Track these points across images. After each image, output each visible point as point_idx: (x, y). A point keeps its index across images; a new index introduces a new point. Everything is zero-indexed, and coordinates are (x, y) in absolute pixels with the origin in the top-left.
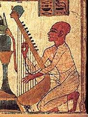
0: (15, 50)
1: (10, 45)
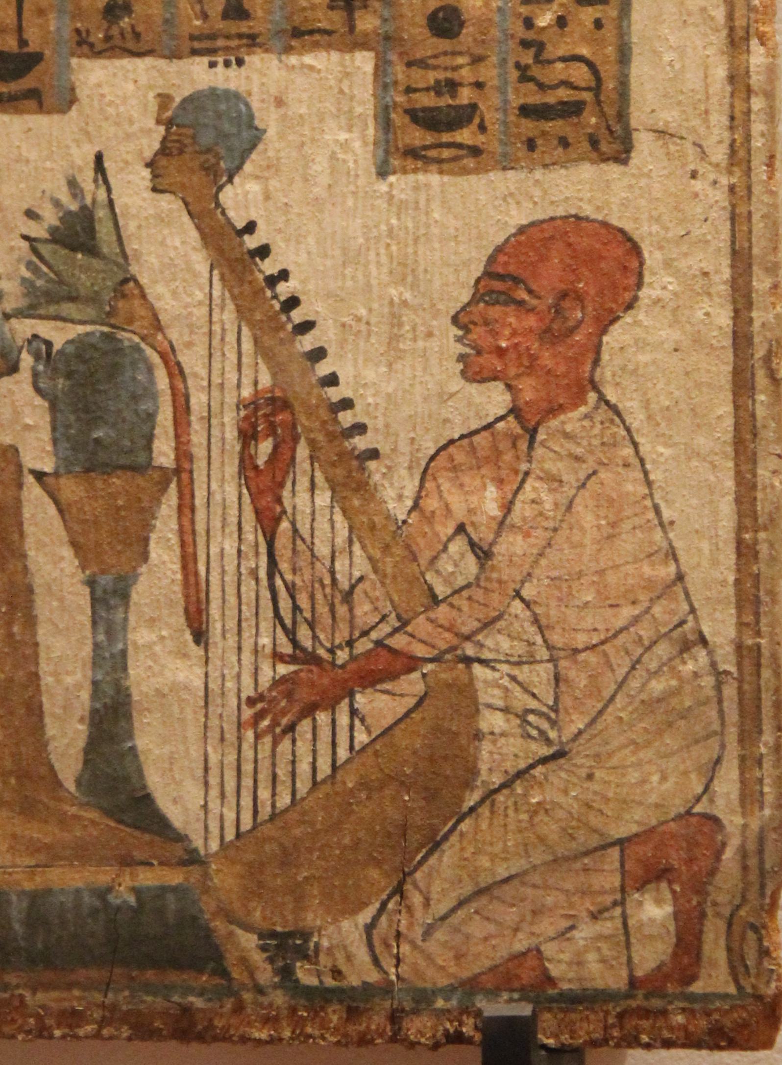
0: (183, 454)
1: (151, 417)
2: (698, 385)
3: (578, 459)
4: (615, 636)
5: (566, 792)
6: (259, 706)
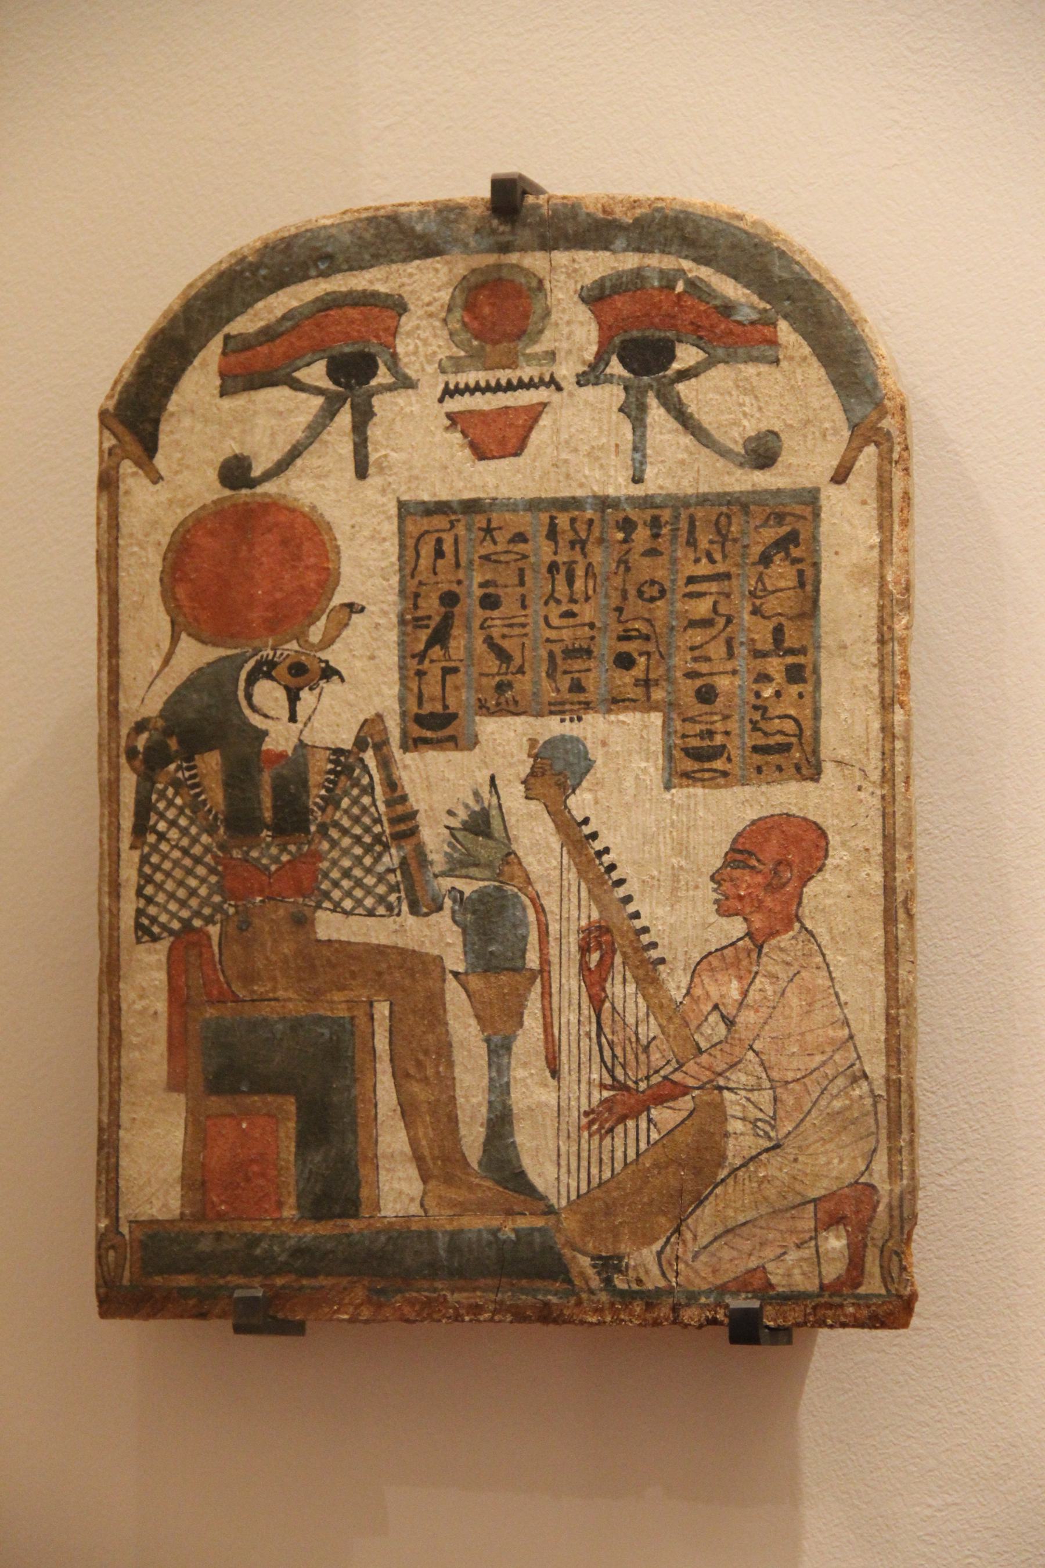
0: (544, 961)
1: (525, 938)
2: (862, 918)
3: (788, 964)
4: (811, 1073)
5: (781, 1170)
6: (592, 1116)
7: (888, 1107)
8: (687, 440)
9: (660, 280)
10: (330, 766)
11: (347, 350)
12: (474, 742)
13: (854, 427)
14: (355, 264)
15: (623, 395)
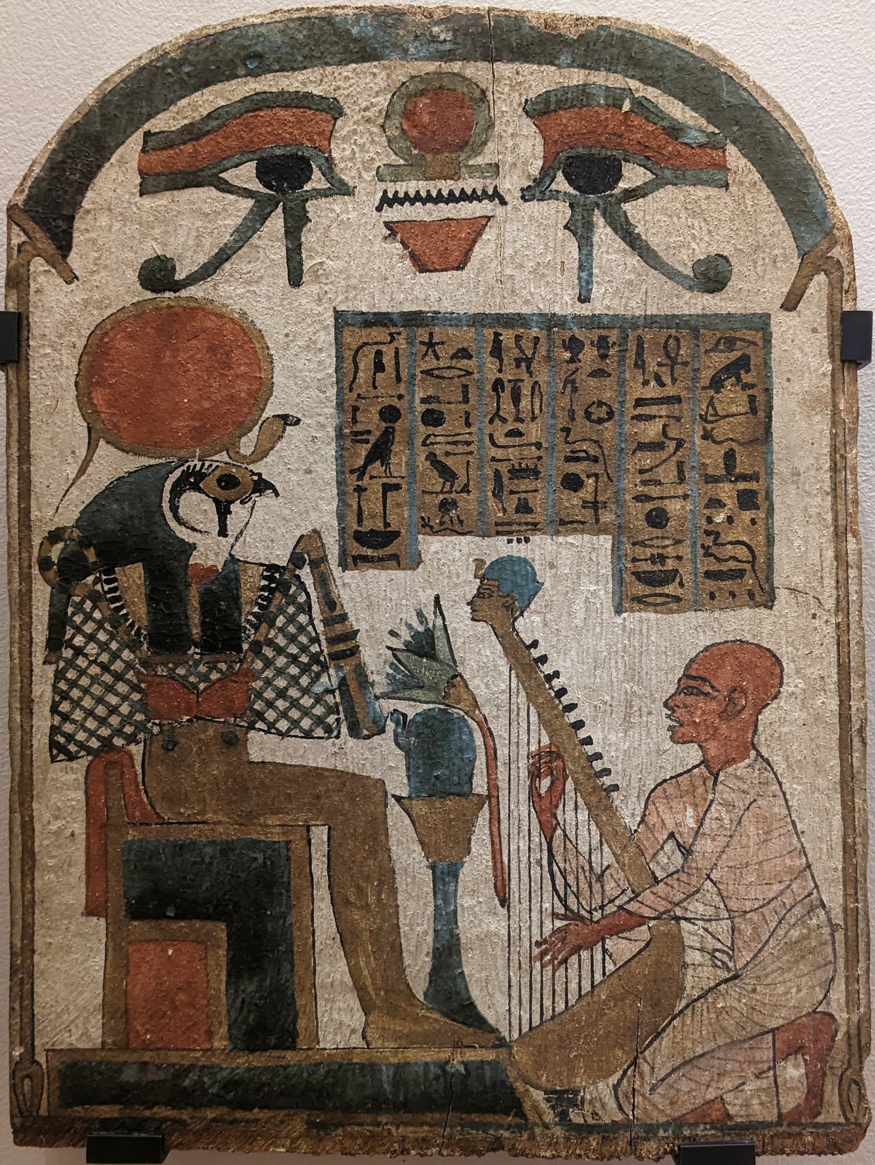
0: (493, 786)
1: (472, 762)
2: (818, 747)
4: (769, 903)
5: (740, 1001)
6: (544, 947)
7: (846, 935)
8: (634, 261)
9: (606, 98)
10: (264, 583)
11: (278, 152)
12: (416, 562)
13: (803, 256)
14: (286, 65)
15: (569, 212)
